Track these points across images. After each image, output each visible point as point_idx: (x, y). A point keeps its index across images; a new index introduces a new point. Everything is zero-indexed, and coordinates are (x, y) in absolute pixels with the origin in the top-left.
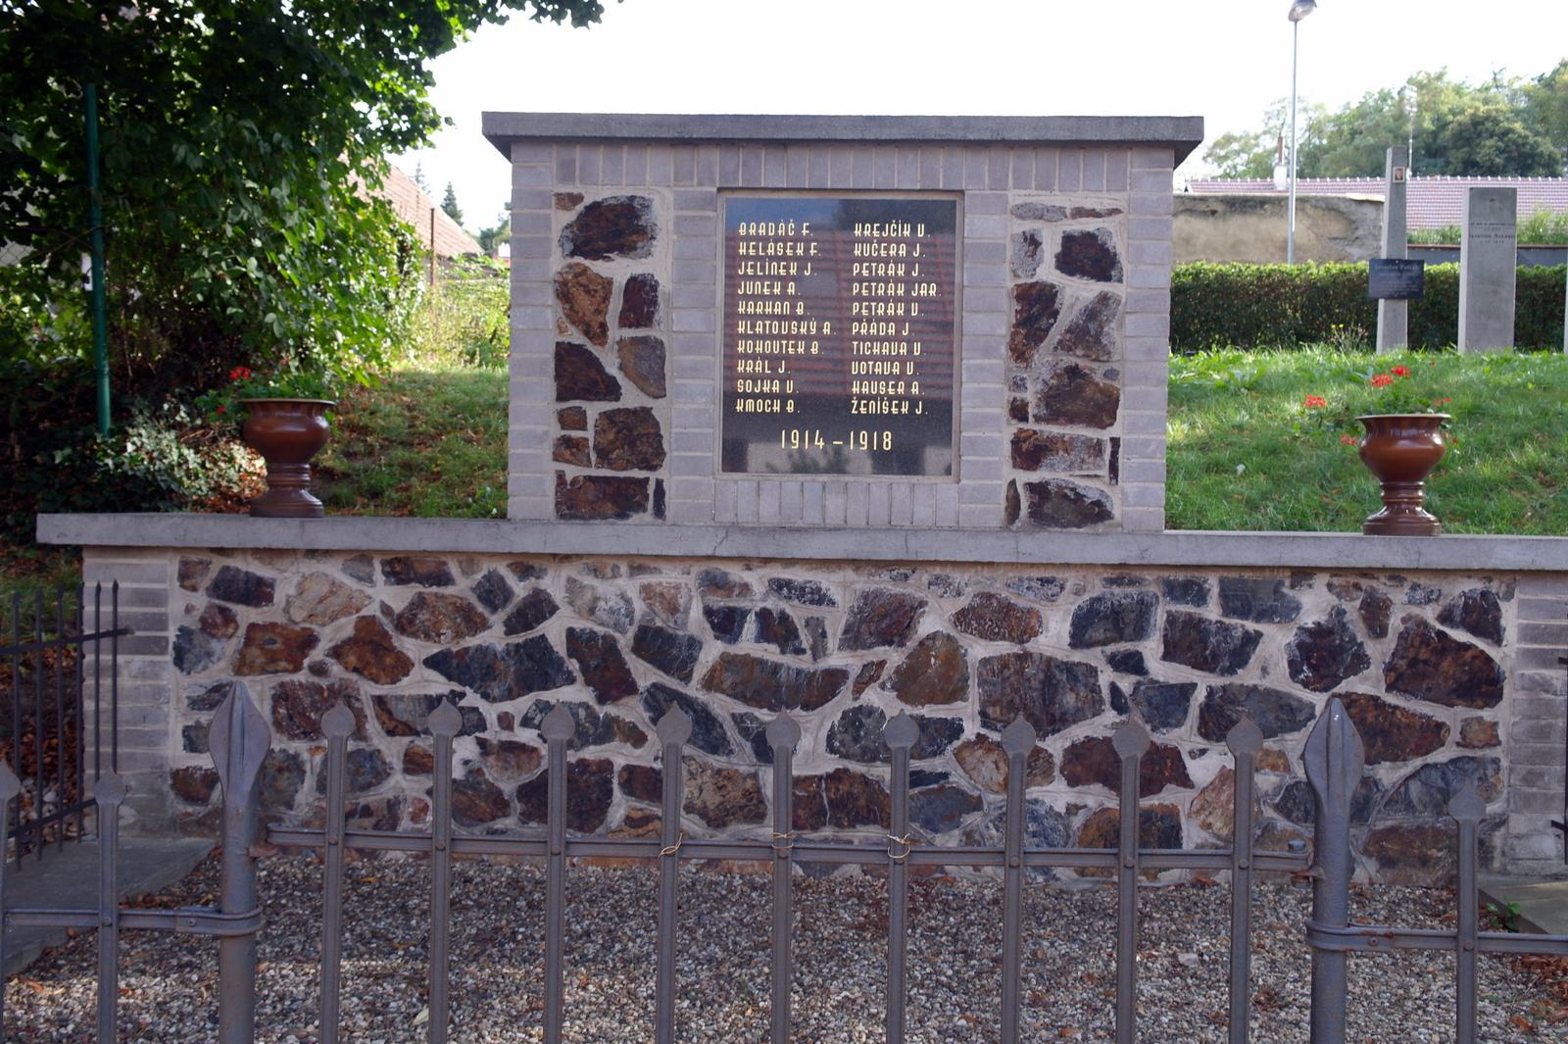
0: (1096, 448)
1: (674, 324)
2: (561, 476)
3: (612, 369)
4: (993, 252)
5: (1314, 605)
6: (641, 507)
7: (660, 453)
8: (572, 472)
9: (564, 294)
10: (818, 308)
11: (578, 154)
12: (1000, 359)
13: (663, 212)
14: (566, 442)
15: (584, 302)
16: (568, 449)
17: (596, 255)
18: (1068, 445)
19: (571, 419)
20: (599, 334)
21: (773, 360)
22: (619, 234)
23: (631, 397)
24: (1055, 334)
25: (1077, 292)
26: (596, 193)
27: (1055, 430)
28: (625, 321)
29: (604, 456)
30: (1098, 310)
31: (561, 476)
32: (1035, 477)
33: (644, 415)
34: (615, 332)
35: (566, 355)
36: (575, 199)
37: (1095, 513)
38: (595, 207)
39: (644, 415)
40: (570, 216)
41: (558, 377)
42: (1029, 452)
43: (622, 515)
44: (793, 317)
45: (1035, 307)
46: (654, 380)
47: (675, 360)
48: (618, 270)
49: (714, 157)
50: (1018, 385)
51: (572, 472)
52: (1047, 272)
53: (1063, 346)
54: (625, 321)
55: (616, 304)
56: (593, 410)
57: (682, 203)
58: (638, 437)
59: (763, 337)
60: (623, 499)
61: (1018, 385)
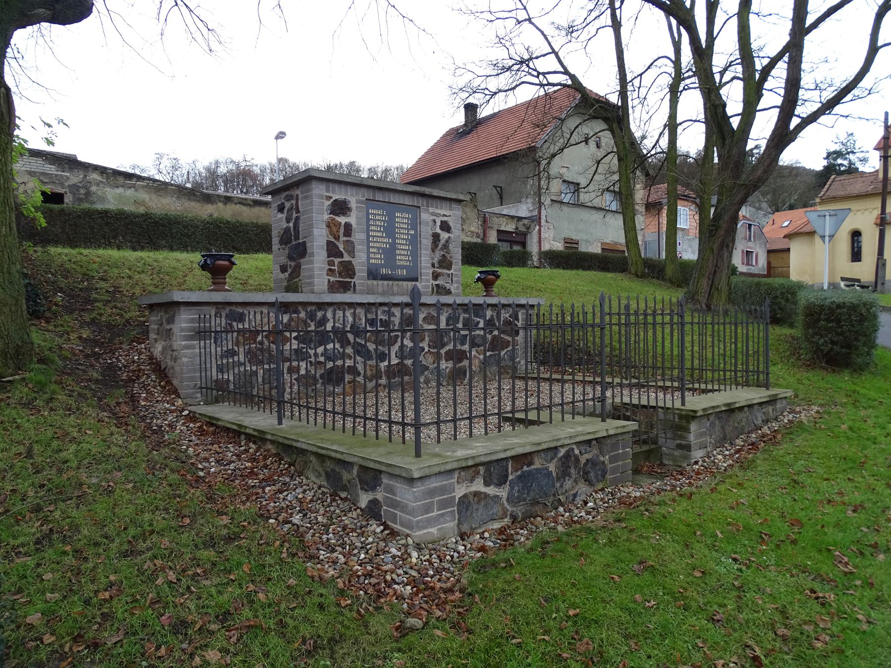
0: (449, 275)
1: (358, 236)
2: (329, 280)
3: (341, 249)
4: (427, 224)
5: (489, 313)
6: (350, 290)
7: (355, 274)
8: (332, 279)
9: (328, 226)
10: (387, 236)
11: (331, 185)
12: (429, 252)
13: (353, 204)
14: (330, 270)
15: (334, 229)
16: (331, 272)
17: (336, 215)
18: (443, 275)
19: (331, 263)
20: (337, 238)
21: (379, 248)
22: (343, 209)
23: (346, 258)
24: (440, 246)
25: (444, 236)
26: (335, 197)
27: (439, 270)
28: (345, 235)
29: (340, 275)
30: (448, 241)
31: (329, 280)
32: (437, 283)
33: (350, 263)
34: (342, 238)
35: (329, 243)
36: (331, 198)
37: (449, 292)
38: (336, 200)
39: (350, 263)
40: (329, 203)
41: (327, 250)
42: (436, 276)
43: (345, 292)
44: (382, 237)
45: (436, 237)
46: (352, 253)
47: (358, 247)
48: (342, 220)
49: (364, 190)
50: (433, 259)
51: (332, 279)
52: (438, 230)
53: (442, 249)
54: (345, 235)
55: (342, 230)
56: (337, 261)
57: (358, 202)
58: (348, 270)
59: (377, 242)
60: (345, 287)
61: (433, 259)
